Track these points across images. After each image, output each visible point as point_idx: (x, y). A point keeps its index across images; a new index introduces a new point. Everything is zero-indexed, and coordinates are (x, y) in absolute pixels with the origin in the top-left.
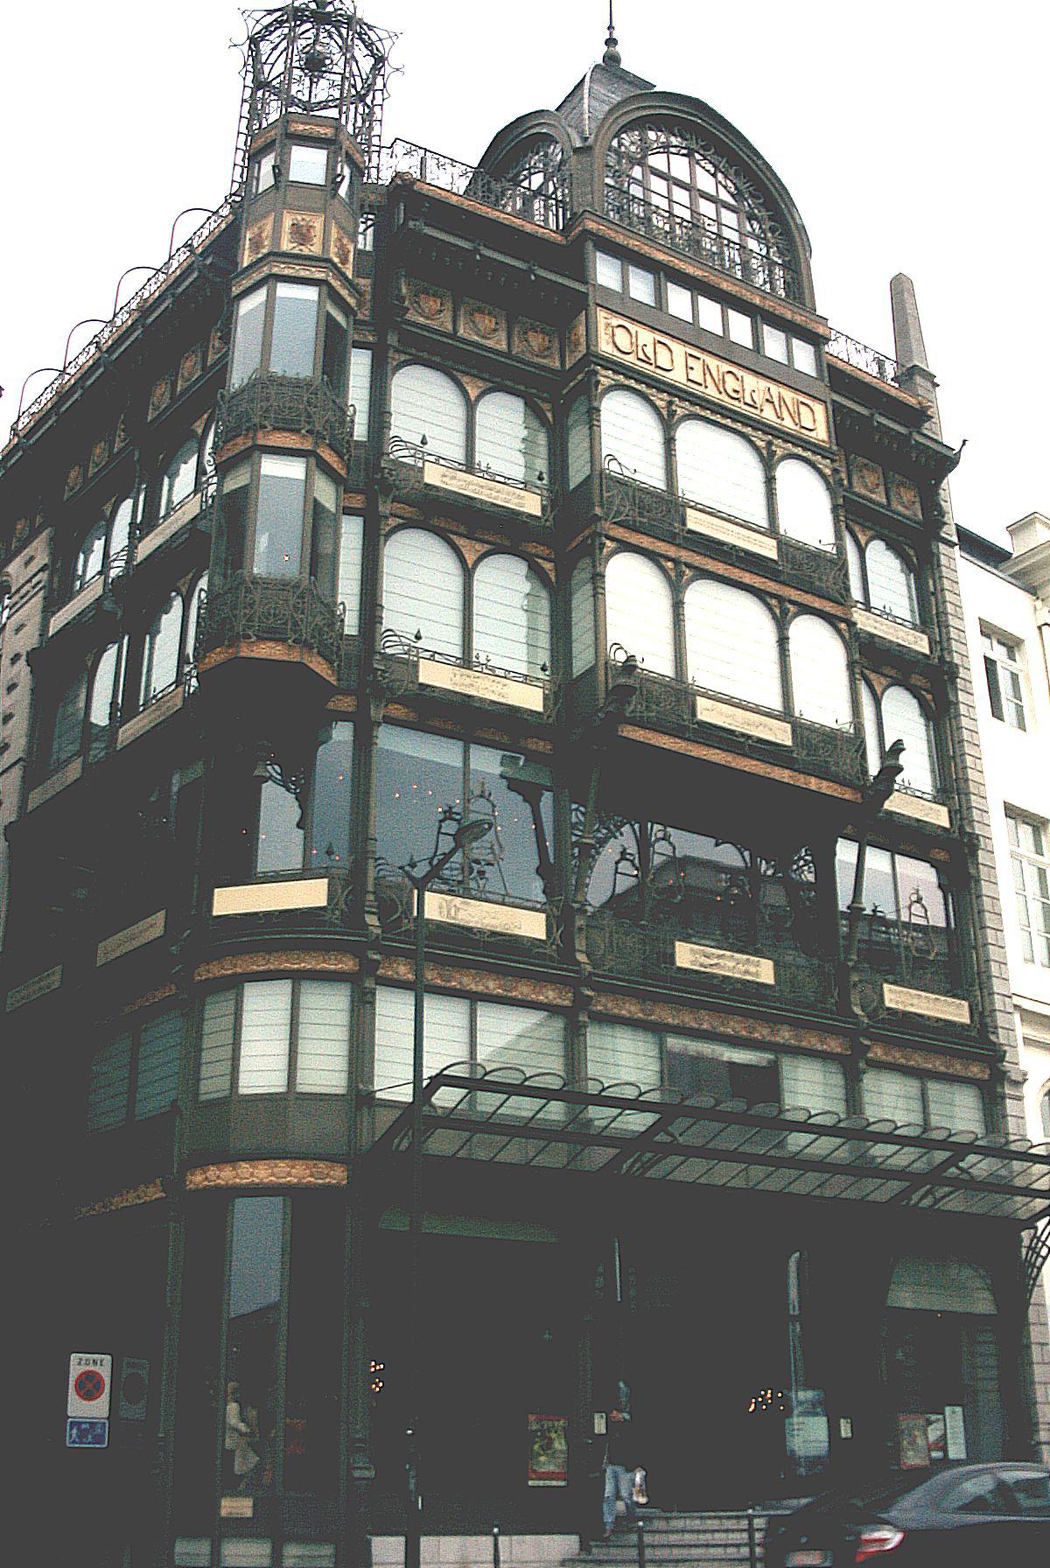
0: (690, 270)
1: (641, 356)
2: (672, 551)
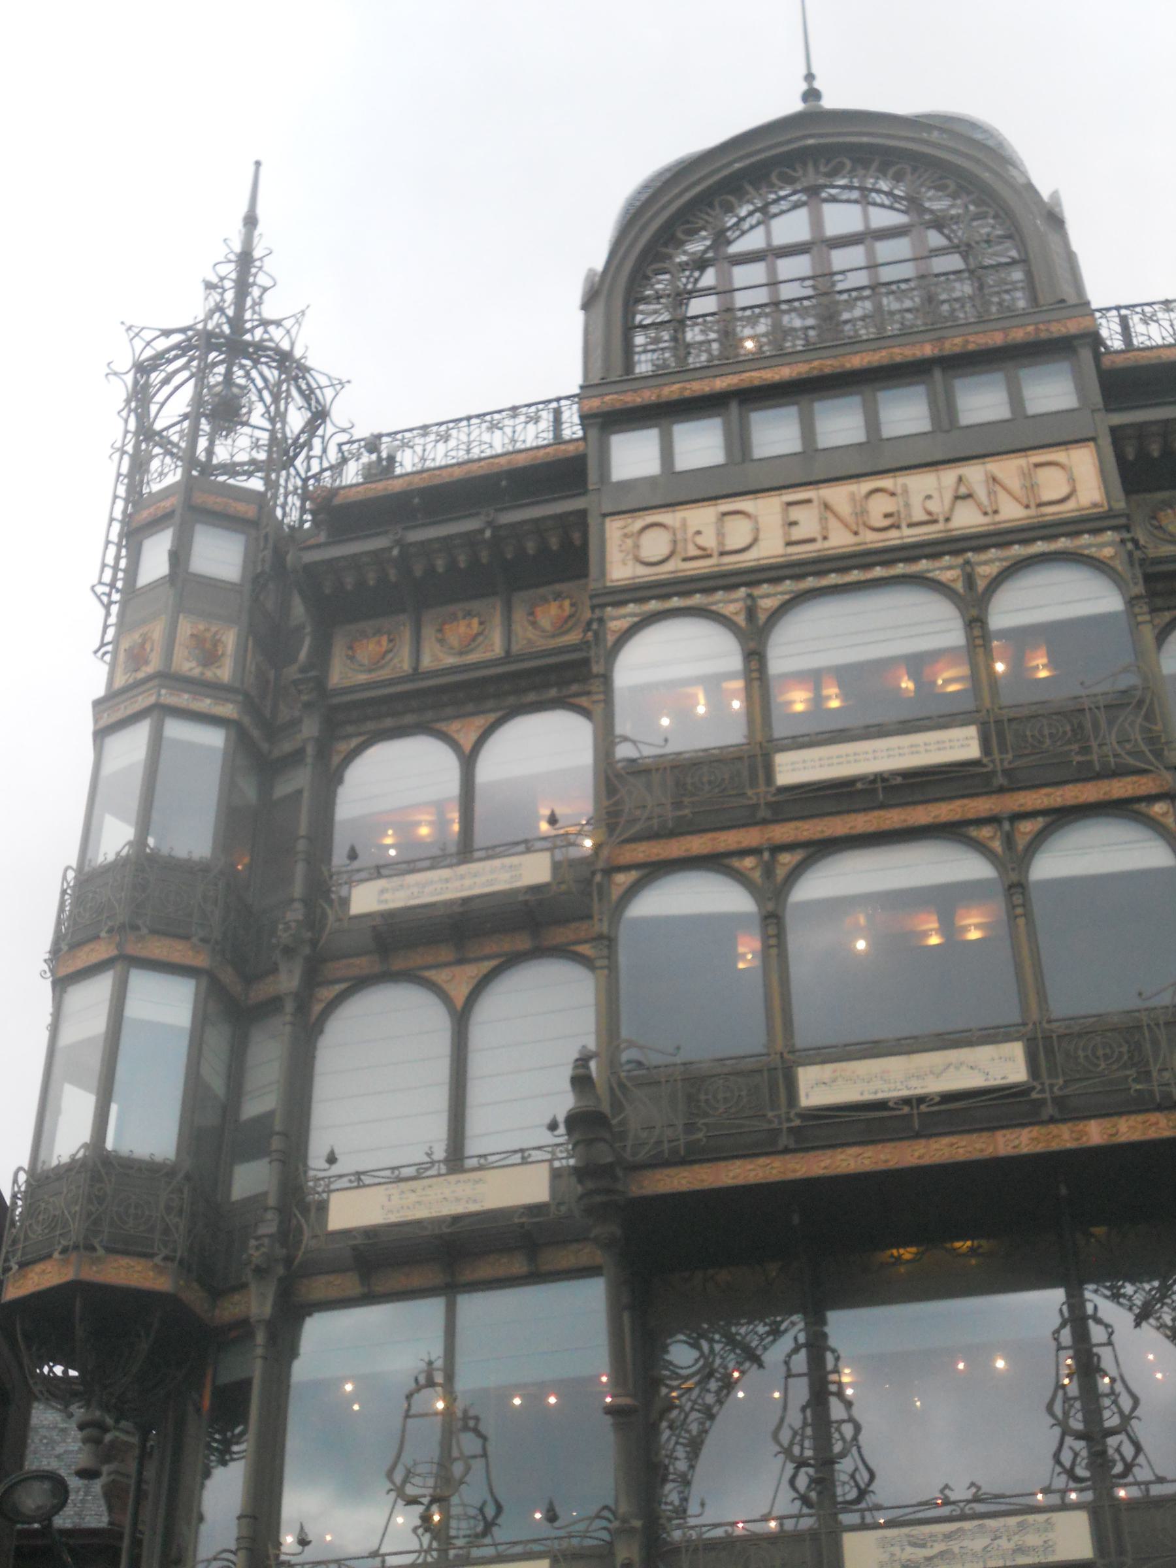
0: (785, 373)
1: (693, 551)
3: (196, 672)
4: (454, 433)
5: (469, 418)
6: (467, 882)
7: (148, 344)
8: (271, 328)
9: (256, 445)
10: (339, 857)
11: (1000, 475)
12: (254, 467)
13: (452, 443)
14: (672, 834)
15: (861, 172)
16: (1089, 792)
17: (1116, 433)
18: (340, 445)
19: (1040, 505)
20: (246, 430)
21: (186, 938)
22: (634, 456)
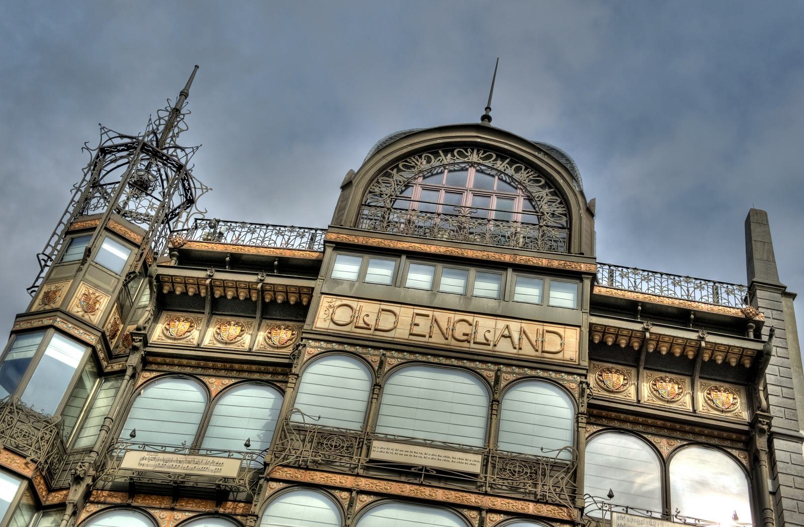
2: (348, 482)
3: (80, 314)
4: (258, 230)
5: (268, 226)
6: (191, 466)
7: (110, 139)
8: (179, 151)
9: (151, 207)
10: (125, 434)
11: (527, 331)
12: (147, 218)
13: (255, 235)
14: (307, 469)
15: (499, 162)
16: (531, 508)
17: (592, 328)
18: (196, 219)
19: (543, 352)
20: (149, 198)
21: (24, 457)
22: (345, 269)
